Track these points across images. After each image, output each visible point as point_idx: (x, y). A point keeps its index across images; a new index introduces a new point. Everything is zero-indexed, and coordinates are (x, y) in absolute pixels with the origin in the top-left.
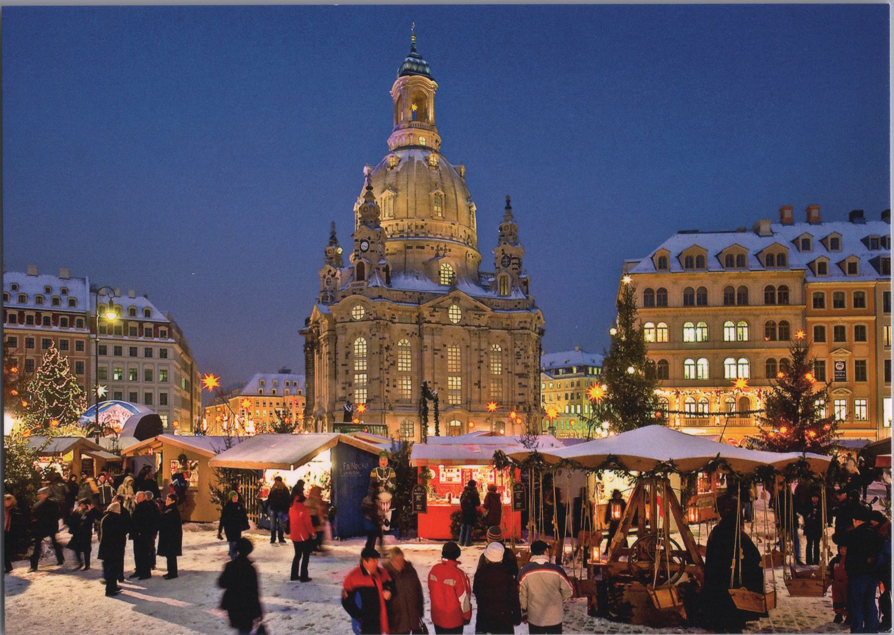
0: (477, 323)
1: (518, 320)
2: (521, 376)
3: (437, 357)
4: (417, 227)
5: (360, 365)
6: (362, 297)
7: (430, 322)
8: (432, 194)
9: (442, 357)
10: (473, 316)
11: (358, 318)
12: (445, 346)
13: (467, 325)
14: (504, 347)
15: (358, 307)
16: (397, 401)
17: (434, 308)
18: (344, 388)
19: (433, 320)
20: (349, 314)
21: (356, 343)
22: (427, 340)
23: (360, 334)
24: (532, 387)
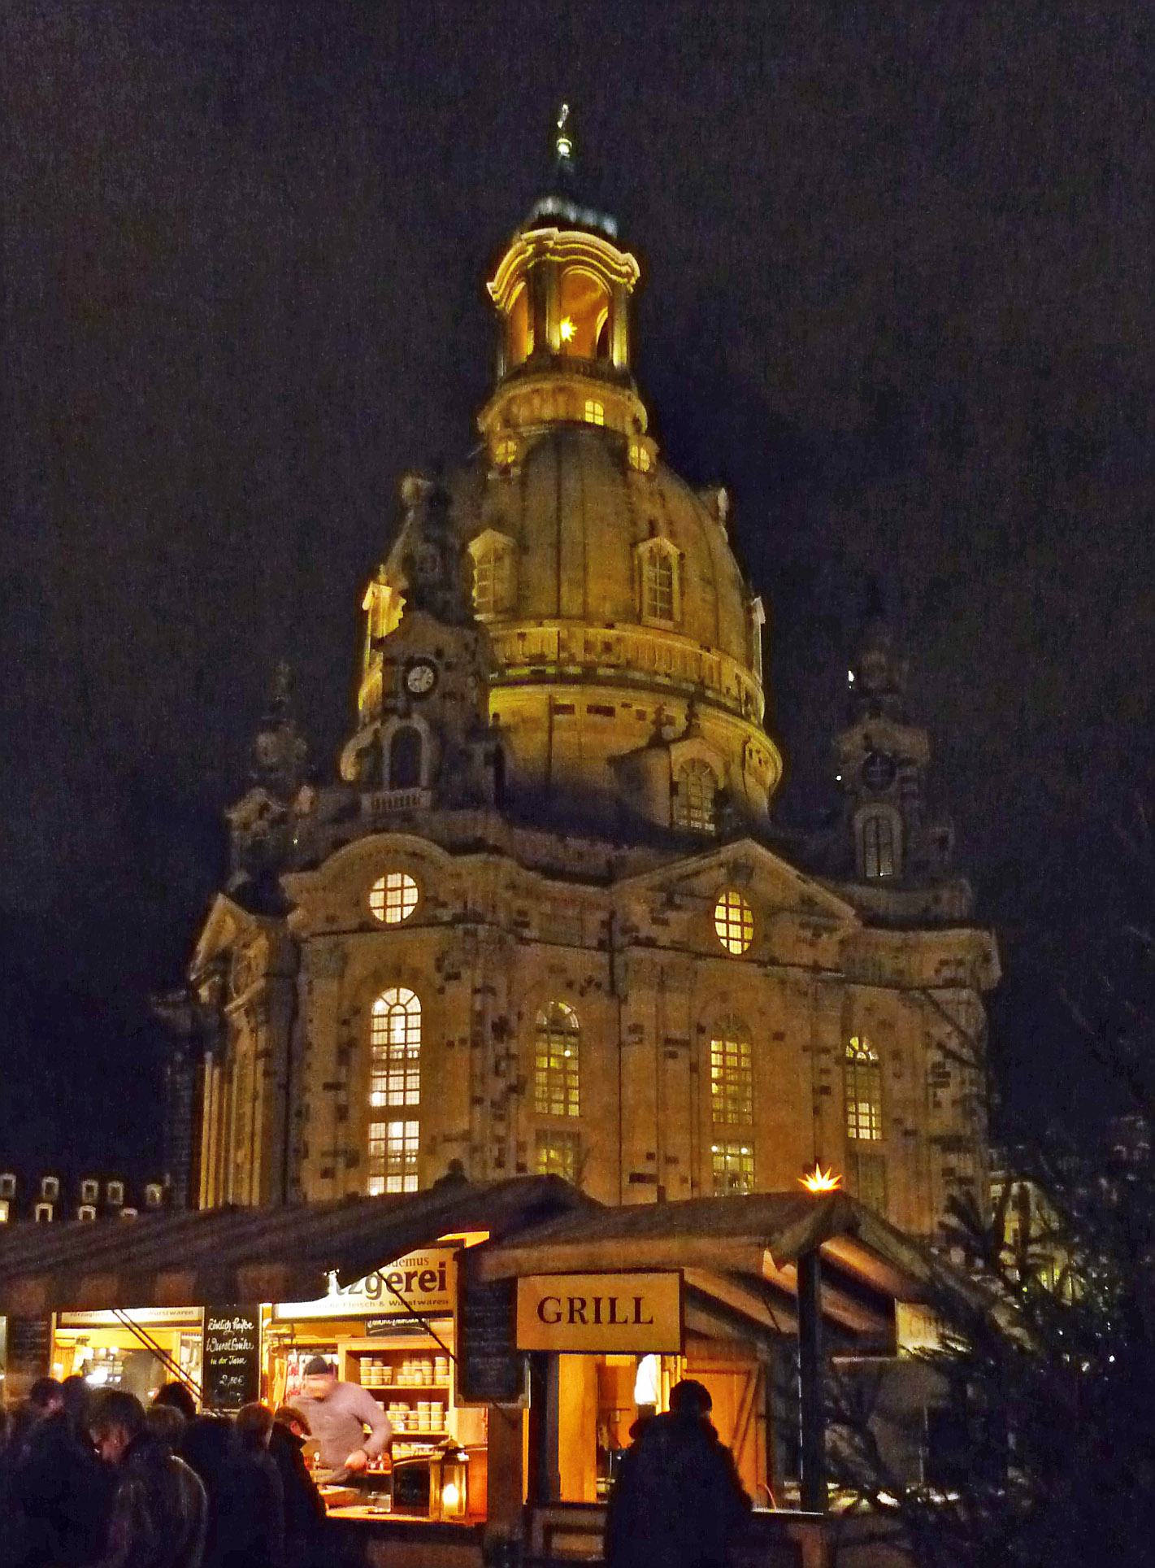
0: (806, 956)
4: (588, 646)
6: (410, 840)
7: (650, 943)
9: (693, 1068)
11: (394, 917)
12: (701, 1030)
13: (774, 961)
15: (394, 880)
17: (670, 897)
18: (327, 1173)
19: (663, 936)
20: (360, 902)
21: (379, 1007)
22: (641, 1005)
23: (397, 976)
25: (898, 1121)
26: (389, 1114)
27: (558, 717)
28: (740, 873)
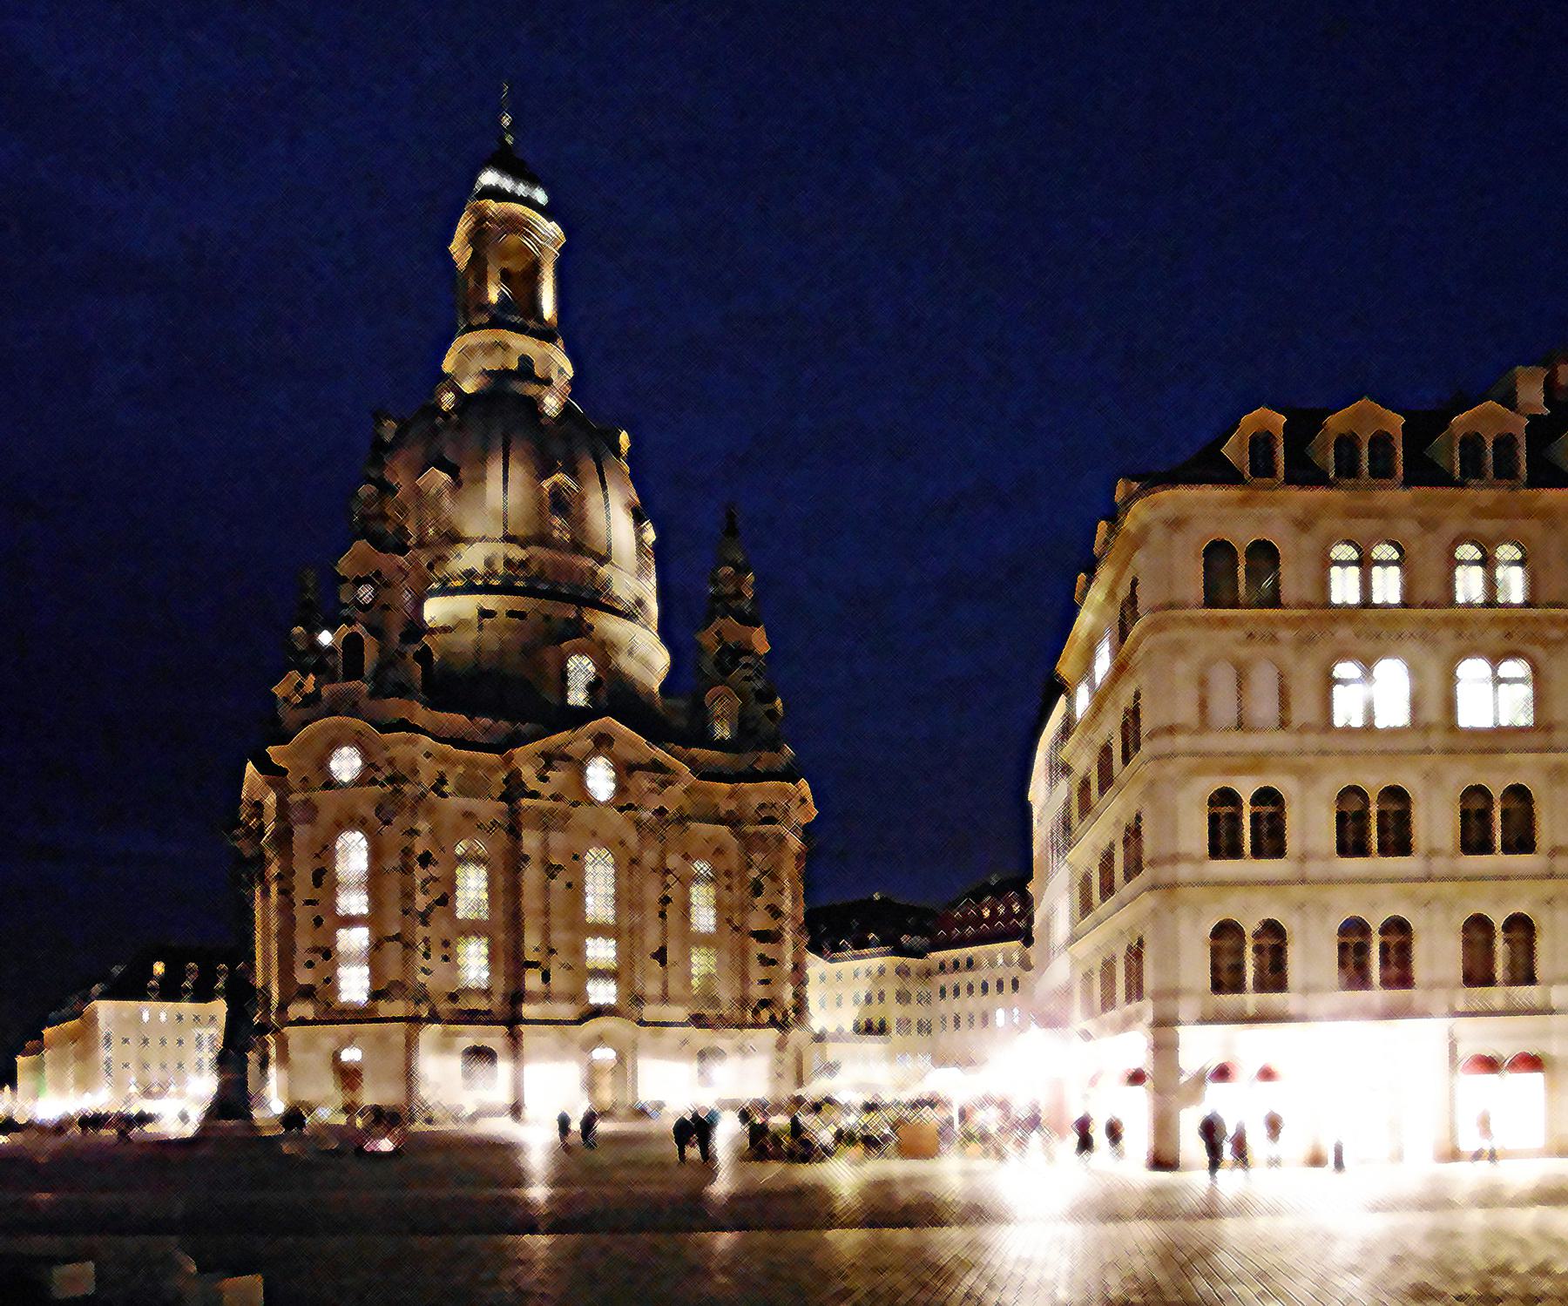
1: (755, 801)
2: (763, 936)
3: (558, 884)
5: (354, 902)
7: (534, 795)
8: (546, 484)
10: (646, 784)
12: (576, 857)
13: (630, 807)
14: (723, 867)
16: (453, 997)
17: (549, 759)
18: (310, 965)
19: (546, 789)
22: (530, 841)
24: (789, 966)
25: (729, 921)
26: (350, 921)
27: (487, 621)
28: (602, 743)
